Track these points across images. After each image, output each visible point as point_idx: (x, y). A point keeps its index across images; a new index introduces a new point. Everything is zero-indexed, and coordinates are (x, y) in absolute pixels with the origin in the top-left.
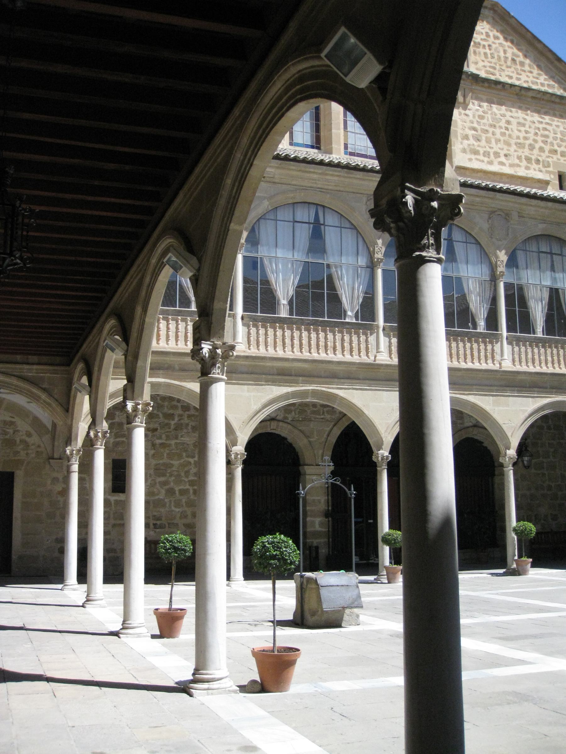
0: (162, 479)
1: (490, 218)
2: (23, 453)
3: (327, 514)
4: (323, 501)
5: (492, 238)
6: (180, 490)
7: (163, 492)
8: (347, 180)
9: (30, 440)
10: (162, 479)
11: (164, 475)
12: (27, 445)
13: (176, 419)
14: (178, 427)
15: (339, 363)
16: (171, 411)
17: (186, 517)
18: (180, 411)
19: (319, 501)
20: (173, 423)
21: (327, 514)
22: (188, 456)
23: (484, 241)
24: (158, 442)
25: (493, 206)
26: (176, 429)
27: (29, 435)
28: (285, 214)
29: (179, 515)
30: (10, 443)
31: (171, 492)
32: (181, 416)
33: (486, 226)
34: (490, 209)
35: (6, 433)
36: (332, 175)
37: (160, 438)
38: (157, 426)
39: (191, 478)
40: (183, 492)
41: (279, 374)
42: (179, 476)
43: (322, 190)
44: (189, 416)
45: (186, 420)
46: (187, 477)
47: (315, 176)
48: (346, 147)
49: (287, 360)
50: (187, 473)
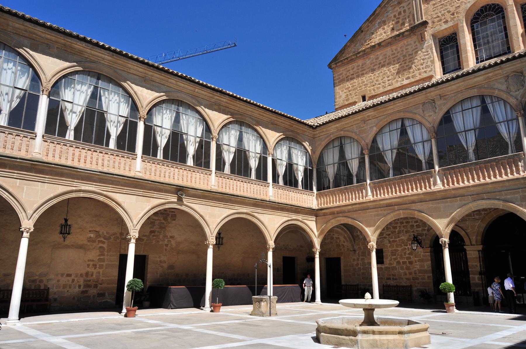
0: (394, 257)
1: (506, 81)
2: (343, 249)
3: (481, 273)
4: (479, 265)
5: (509, 93)
6: (403, 262)
7: (395, 263)
8: (407, 102)
9: (345, 244)
10: (394, 257)
11: (395, 255)
12: (343, 245)
13: (398, 228)
14: (399, 232)
15: (412, 195)
16: (395, 225)
17: (406, 274)
18: (399, 225)
19: (476, 265)
20: (397, 230)
21: (481, 273)
22: (404, 246)
23: (504, 96)
24: (391, 240)
25: (505, 72)
26: (398, 233)
27: (344, 242)
28: (387, 129)
29: (402, 274)
30: (338, 246)
31: (398, 263)
32: (400, 227)
33: (504, 87)
34: (505, 75)
35: (337, 242)
36: (399, 103)
37: (392, 238)
38: (390, 233)
39: (407, 256)
40: (404, 263)
41: (387, 206)
42: (401, 255)
43: (399, 111)
44: (404, 226)
45: (402, 229)
46: (405, 255)
47: (391, 107)
48: (477, 59)
49: (387, 199)
50: (405, 253)
